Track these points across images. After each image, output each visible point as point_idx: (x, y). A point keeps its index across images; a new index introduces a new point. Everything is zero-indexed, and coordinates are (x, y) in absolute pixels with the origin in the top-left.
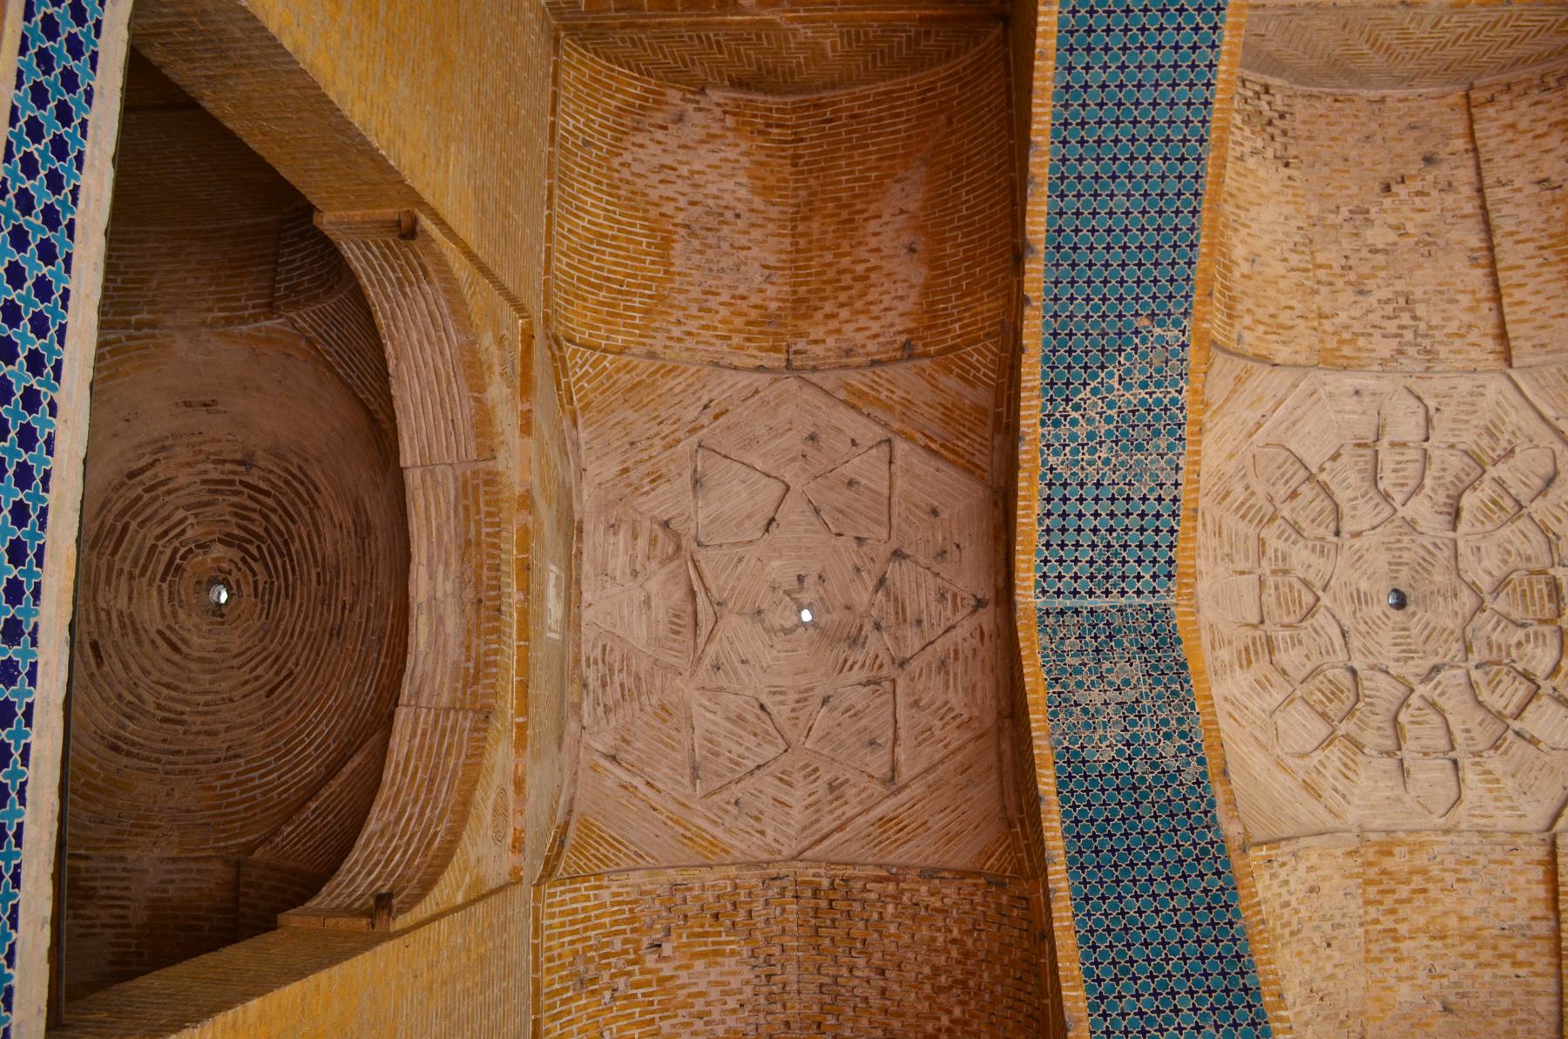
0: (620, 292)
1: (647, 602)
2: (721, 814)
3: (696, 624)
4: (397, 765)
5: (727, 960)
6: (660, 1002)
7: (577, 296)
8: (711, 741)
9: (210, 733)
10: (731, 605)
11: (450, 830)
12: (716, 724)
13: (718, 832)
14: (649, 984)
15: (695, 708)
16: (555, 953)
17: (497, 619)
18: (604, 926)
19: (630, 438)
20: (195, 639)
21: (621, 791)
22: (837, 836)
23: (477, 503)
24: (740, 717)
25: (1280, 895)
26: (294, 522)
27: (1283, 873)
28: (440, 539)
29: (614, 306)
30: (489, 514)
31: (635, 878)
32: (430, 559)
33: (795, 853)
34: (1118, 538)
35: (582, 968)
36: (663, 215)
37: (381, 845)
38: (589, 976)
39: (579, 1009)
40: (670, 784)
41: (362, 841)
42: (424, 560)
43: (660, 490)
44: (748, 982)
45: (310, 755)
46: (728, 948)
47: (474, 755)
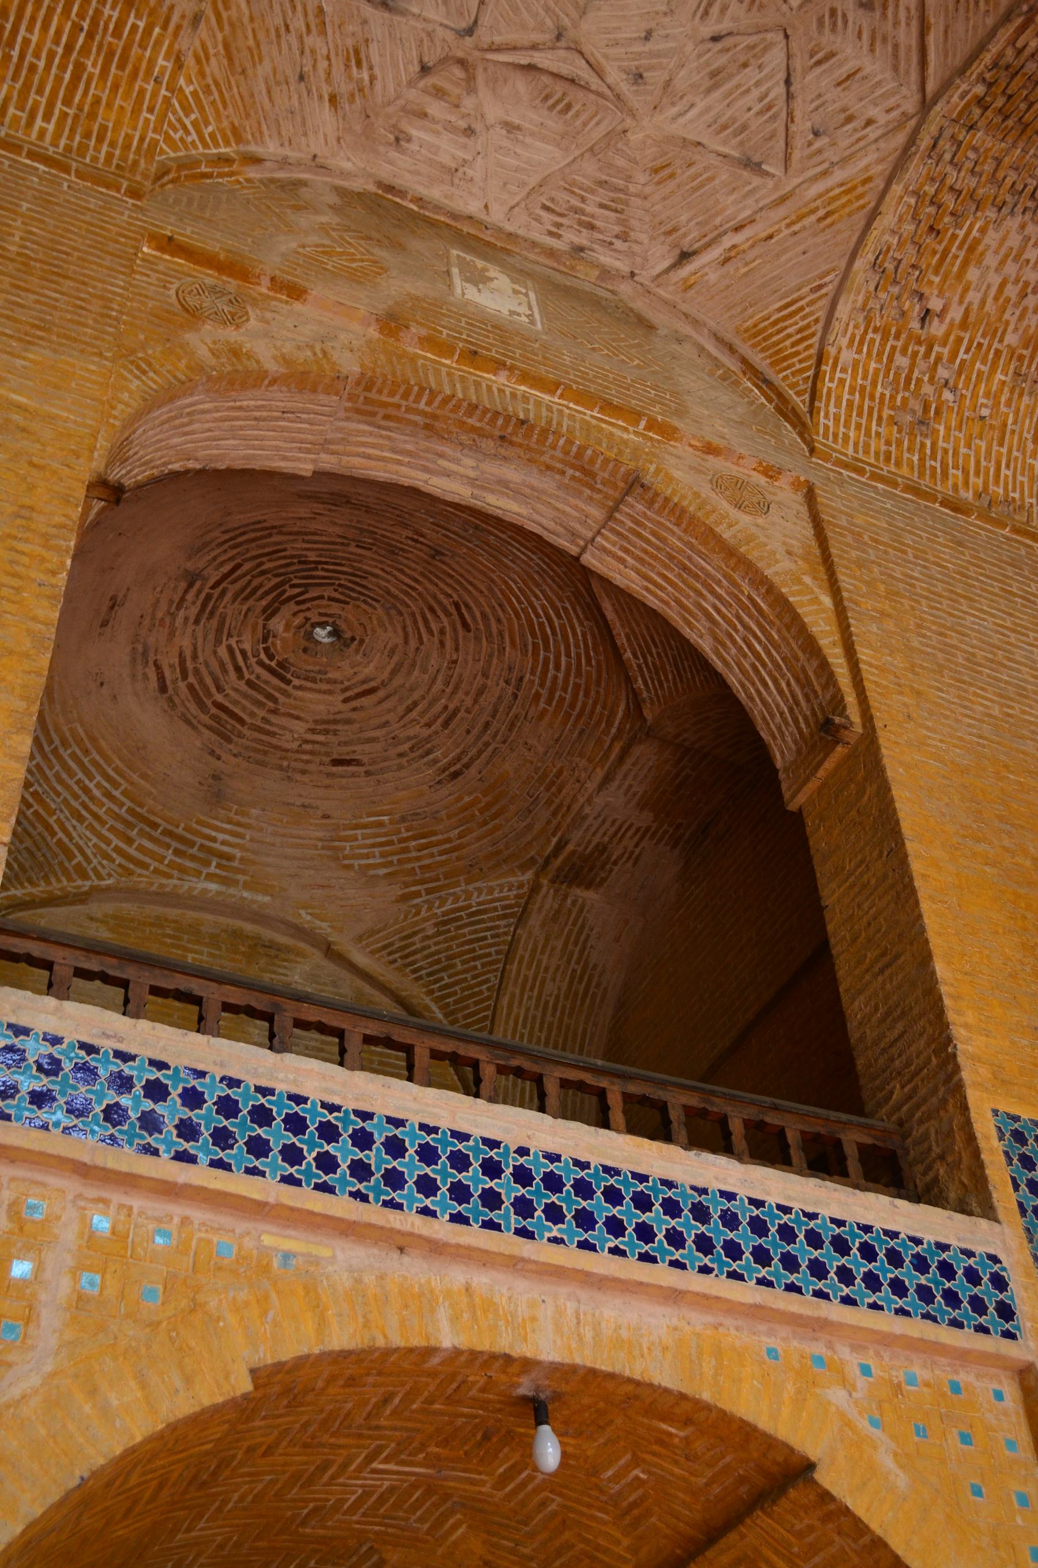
0: (90, 36)
1: (511, 128)
2: (818, 159)
3: (572, 81)
4: (647, 589)
5: (987, 240)
6: (984, 336)
7: (92, 116)
8: (725, 127)
9: (481, 692)
10: (566, 22)
11: (752, 583)
12: (707, 110)
13: (839, 175)
14: (959, 340)
15: (677, 129)
16: (883, 448)
17: (532, 428)
18: (877, 371)
19: (293, 78)
20: (368, 671)
21: (730, 267)
22: (931, 40)
23: (385, 405)
24: (713, 74)
26: (285, 550)
28: (409, 453)
29: (111, 54)
30: (405, 396)
31: (843, 311)
32: (426, 469)
33: (917, 97)
35: (909, 418)
37: (734, 651)
38: (919, 408)
39: (947, 439)
40: (750, 201)
41: (719, 665)
42: (425, 476)
43: (375, 59)
44: (1023, 227)
45: (563, 627)
46: (975, 233)
47: (680, 517)
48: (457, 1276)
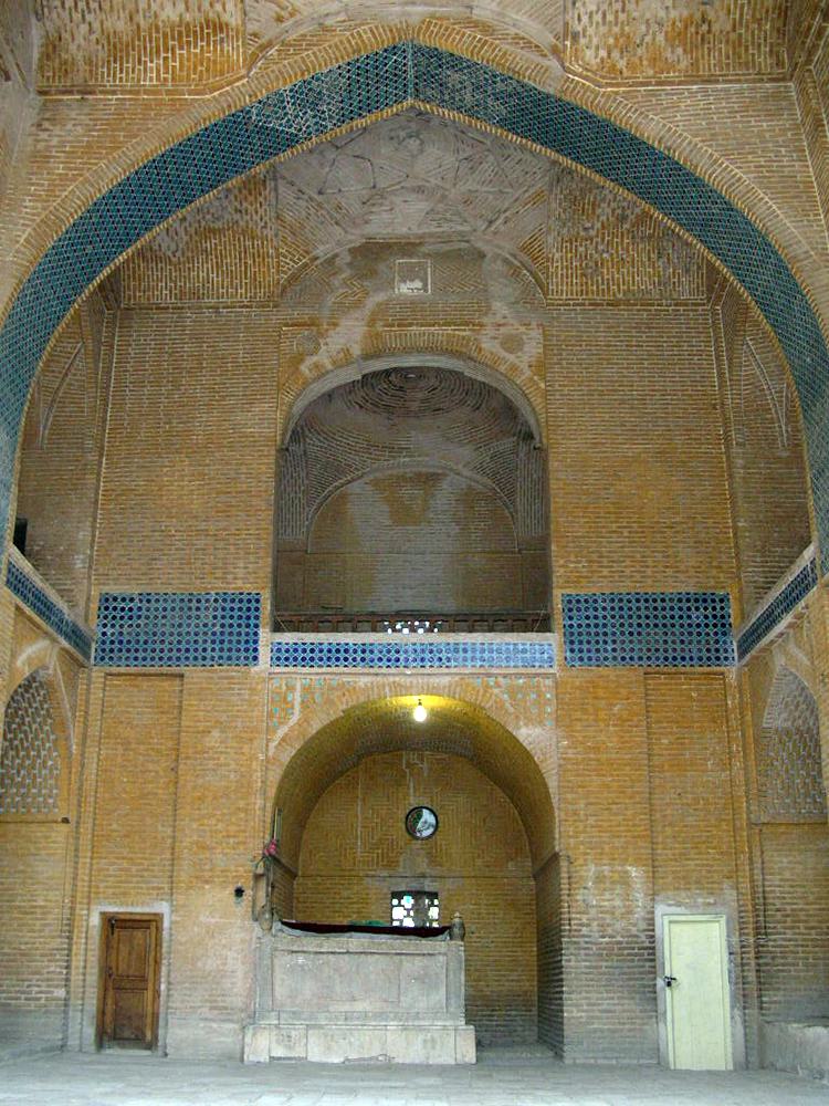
8: (483, 182)
24: (471, 168)
25: (598, 23)
27: (585, 19)
34: (372, 80)
35: (590, 271)
36: (196, 233)
48: (391, 679)
